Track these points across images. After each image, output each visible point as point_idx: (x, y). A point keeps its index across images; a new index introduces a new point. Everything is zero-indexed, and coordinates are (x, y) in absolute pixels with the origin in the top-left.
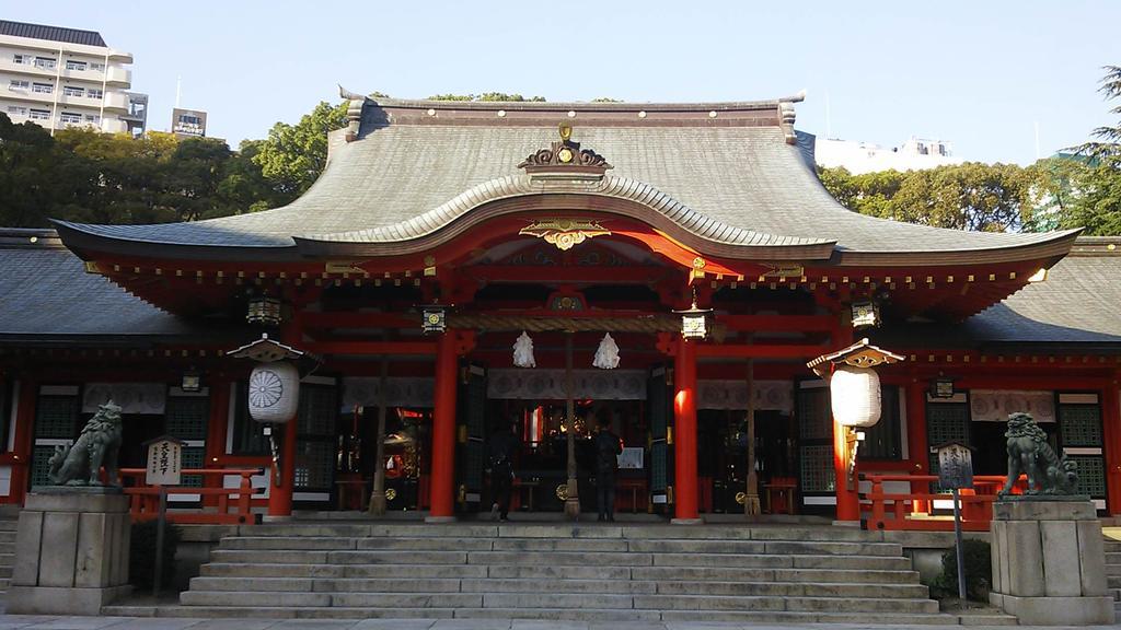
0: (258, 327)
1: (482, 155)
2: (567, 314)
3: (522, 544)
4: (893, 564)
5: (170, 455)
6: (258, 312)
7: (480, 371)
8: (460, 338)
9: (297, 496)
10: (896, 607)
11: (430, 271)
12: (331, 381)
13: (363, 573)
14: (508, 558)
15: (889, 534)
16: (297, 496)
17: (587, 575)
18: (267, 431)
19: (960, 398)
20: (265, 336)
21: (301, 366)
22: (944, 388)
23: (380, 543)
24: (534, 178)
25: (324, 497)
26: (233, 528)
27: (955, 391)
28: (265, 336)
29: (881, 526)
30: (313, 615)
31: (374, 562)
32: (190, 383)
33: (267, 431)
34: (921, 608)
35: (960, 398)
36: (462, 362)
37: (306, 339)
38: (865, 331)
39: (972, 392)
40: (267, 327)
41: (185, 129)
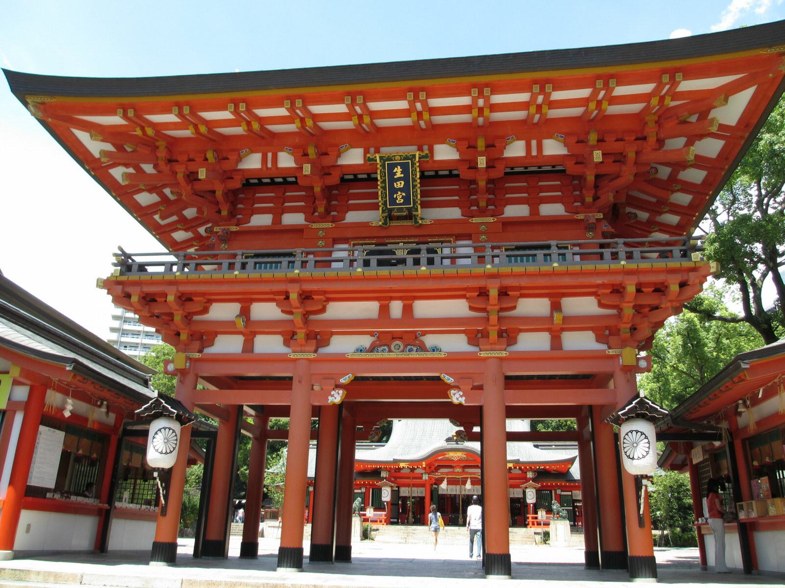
0: (383, 479)
1: (436, 426)
2: (458, 473)
4: (530, 535)
5: (371, 511)
6: (384, 474)
7: (434, 486)
8: (431, 479)
9: (392, 520)
10: (526, 544)
11: (424, 466)
12: (397, 489)
13: (412, 536)
14: (444, 534)
15: (532, 529)
16: (392, 520)
17: (461, 537)
18: (385, 503)
19: (570, 493)
20: (385, 480)
21: (392, 487)
22: (559, 492)
23: (414, 530)
24: (448, 444)
25: (396, 520)
26: (382, 526)
27: (561, 491)
28: (385, 480)
29: (531, 527)
30: (403, 543)
31: (414, 534)
32: (363, 490)
33: (385, 503)
34: (532, 544)
35: (570, 493)
36: (432, 485)
37: (393, 479)
38: (530, 479)
39: (573, 492)
40: (386, 478)
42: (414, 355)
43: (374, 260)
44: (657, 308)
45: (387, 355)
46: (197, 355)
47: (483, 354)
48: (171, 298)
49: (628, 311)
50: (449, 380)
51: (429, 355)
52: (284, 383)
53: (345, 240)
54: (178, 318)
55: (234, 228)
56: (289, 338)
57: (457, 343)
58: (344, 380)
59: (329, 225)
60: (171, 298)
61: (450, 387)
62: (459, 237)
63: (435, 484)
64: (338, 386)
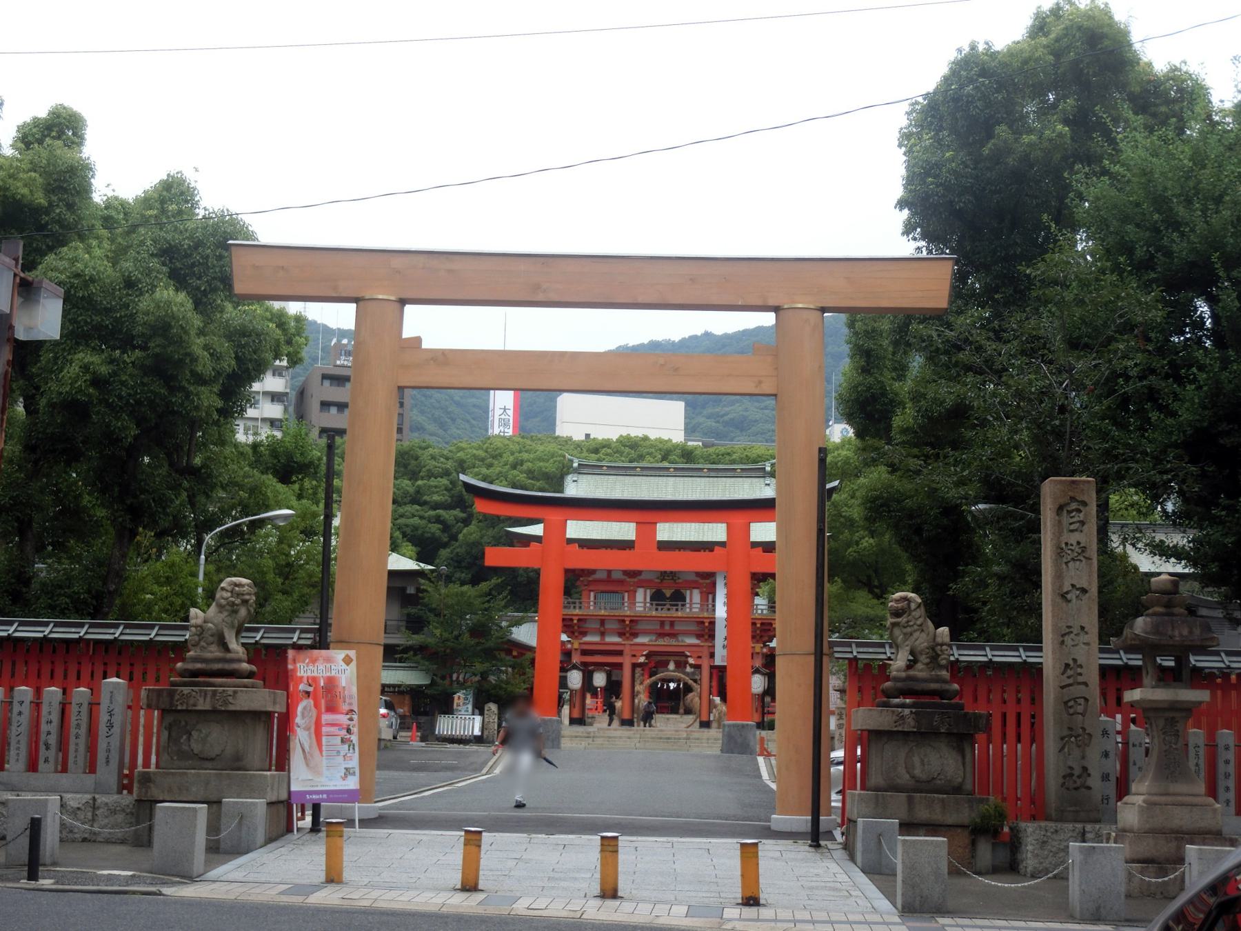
3: (668, 719)
7: (654, 669)
41: (346, 363)
42: (674, 643)
43: (660, 608)
44: (769, 630)
45: (663, 643)
46: (581, 641)
47: (702, 644)
48: (575, 622)
49: (758, 632)
50: (688, 654)
51: (680, 644)
52: (620, 653)
53: (643, 587)
54: (576, 628)
55: (590, 579)
56: (621, 634)
57: (692, 641)
58: (644, 653)
59: (636, 580)
60: (575, 622)
61: (687, 657)
62: (694, 588)
63: (654, 667)
64: (643, 655)
